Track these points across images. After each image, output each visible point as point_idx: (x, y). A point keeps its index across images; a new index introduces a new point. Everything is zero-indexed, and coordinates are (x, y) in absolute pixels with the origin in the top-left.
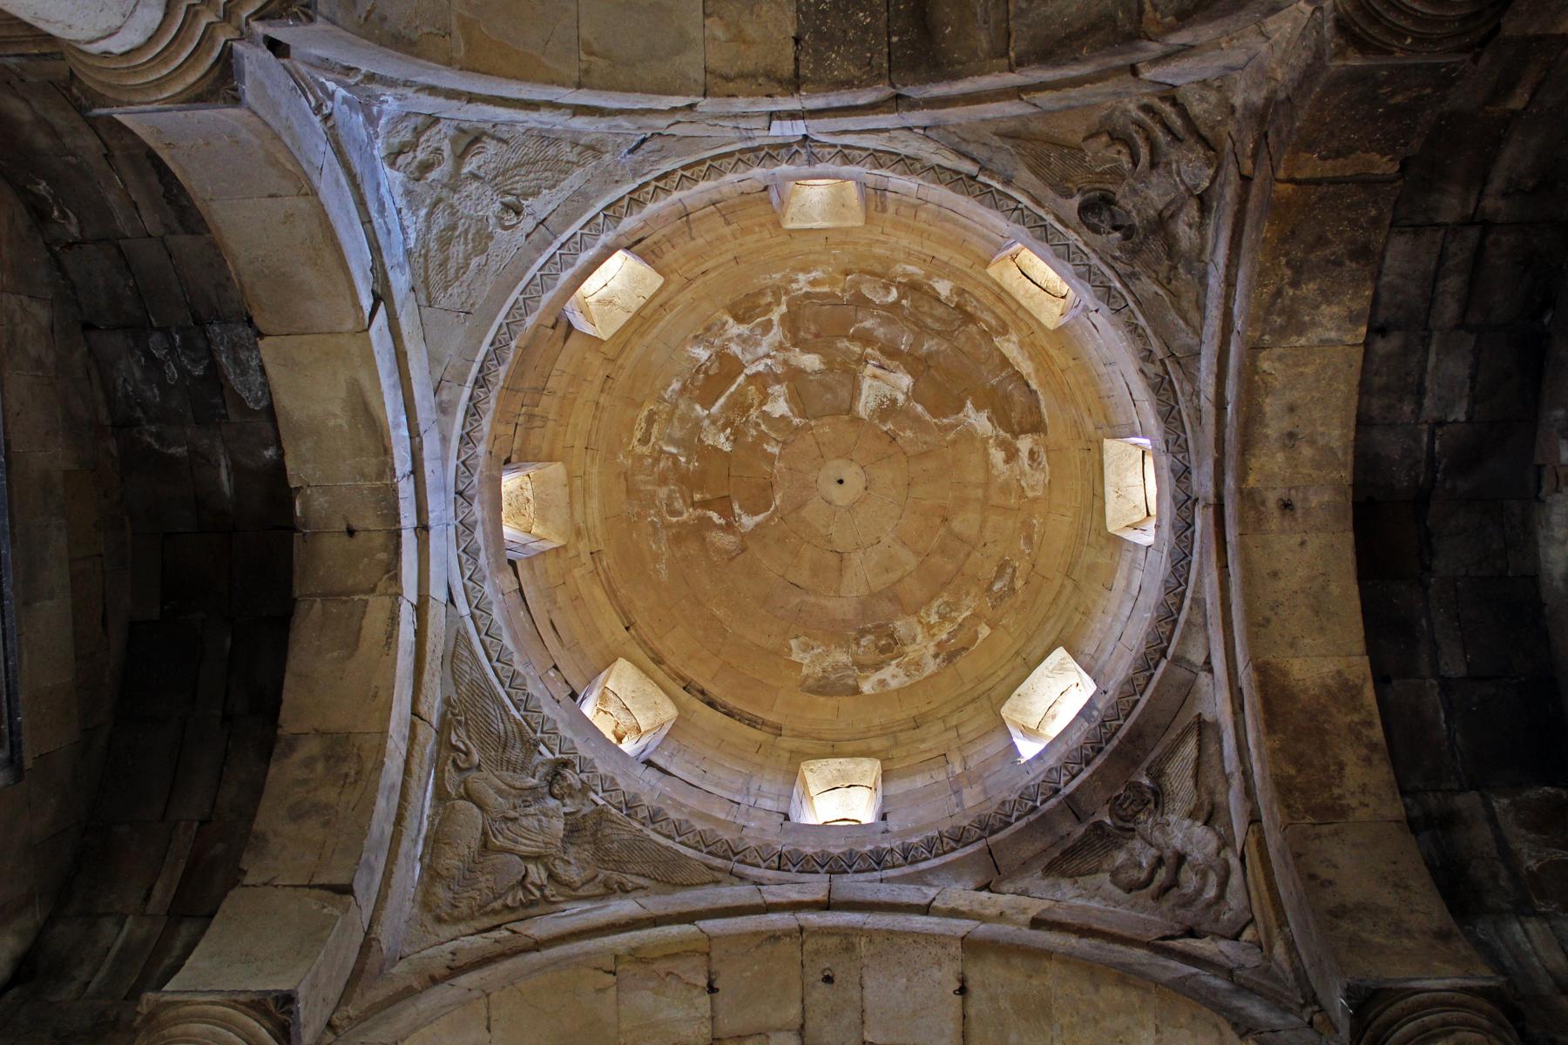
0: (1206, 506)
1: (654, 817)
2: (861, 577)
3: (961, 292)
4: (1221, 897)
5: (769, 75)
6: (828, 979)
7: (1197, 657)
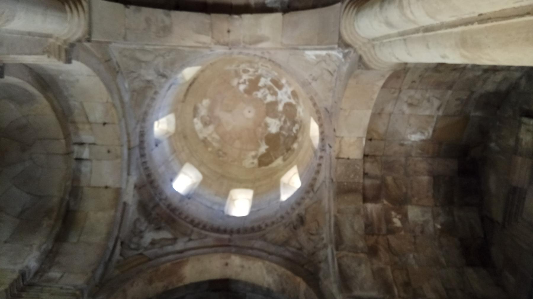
0: (230, 240)
1: (153, 99)
2: (224, 116)
3: (294, 150)
4: (132, 249)
5: (340, 152)
6: (109, 152)
7: (193, 237)
